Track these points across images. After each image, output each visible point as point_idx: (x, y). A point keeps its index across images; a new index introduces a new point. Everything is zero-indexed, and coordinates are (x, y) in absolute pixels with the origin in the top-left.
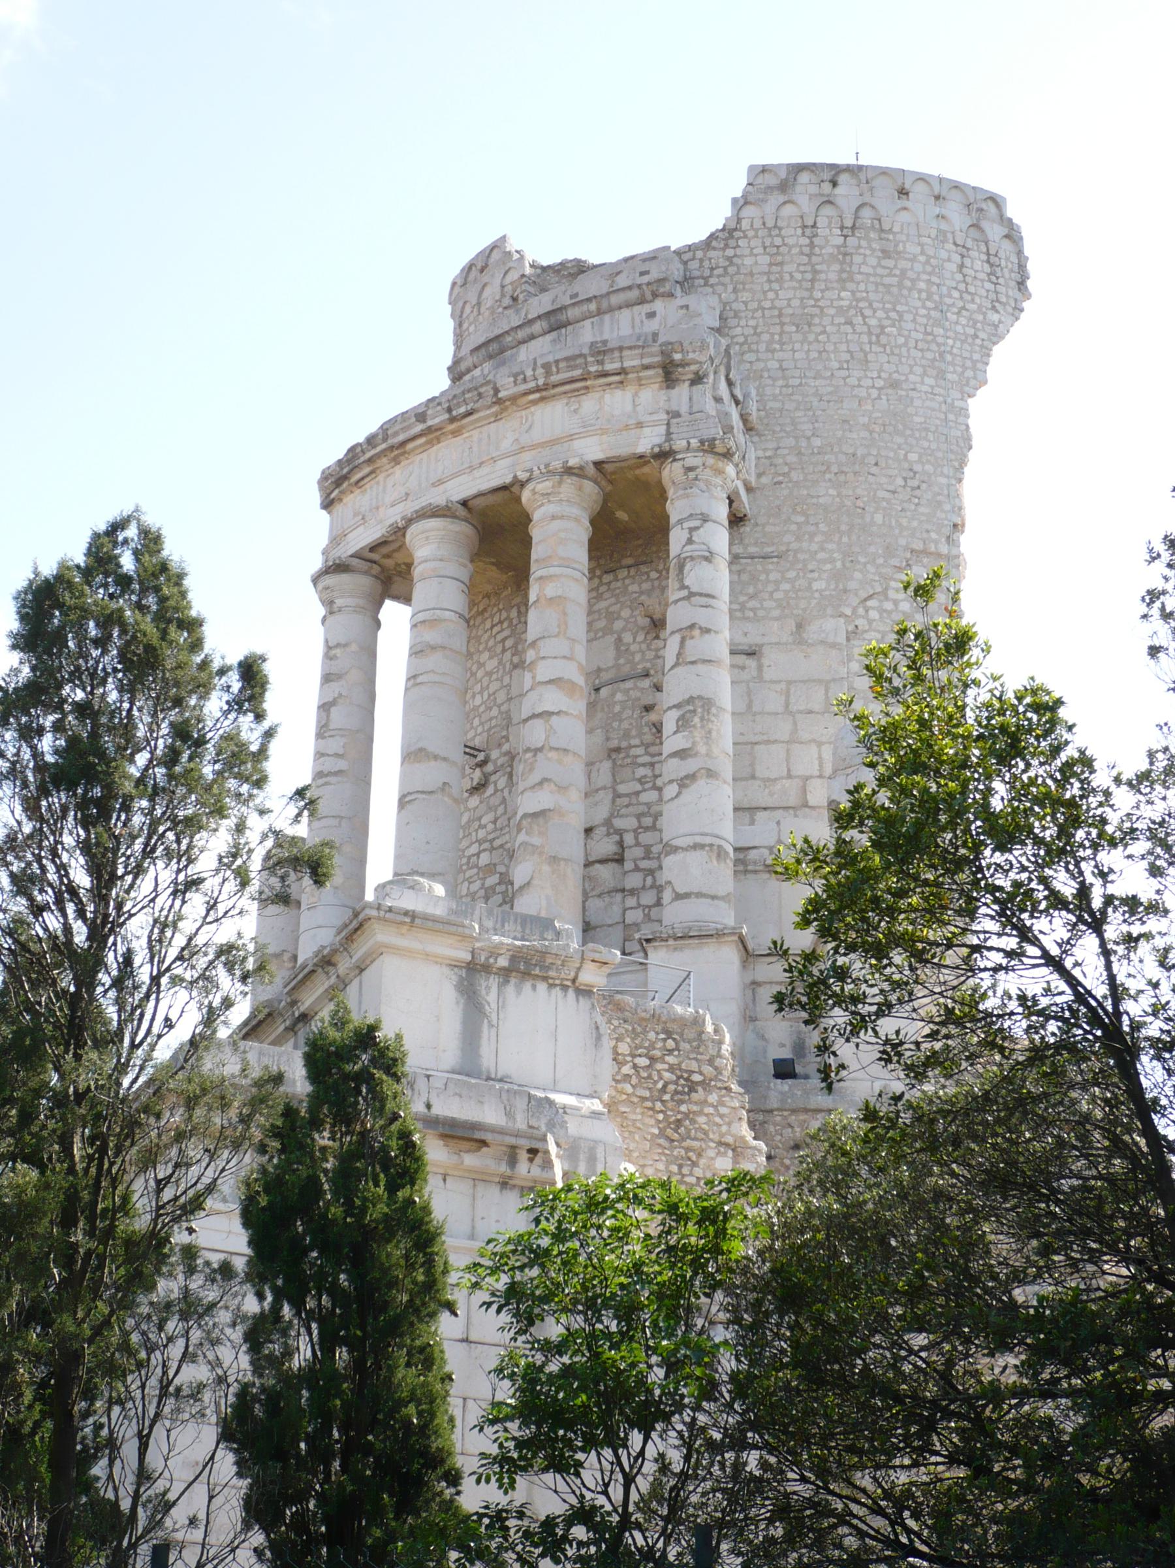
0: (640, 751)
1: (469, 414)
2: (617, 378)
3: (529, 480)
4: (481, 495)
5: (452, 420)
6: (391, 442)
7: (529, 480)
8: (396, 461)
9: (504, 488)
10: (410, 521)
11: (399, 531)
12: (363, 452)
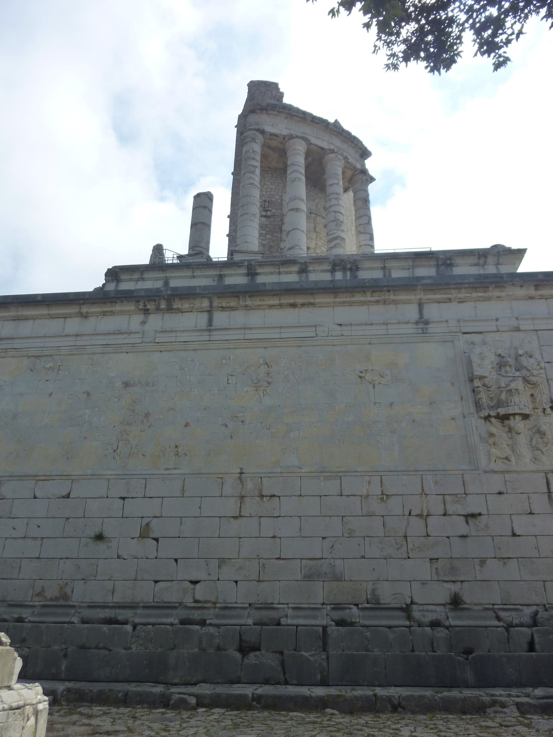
0: (322, 236)
1: (317, 123)
2: (353, 145)
3: (336, 153)
4: (316, 146)
5: (312, 121)
6: (290, 112)
7: (336, 153)
8: (286, 118)
9: (323, 149)
10: (297, 137)
11: (291, 137)
12: (279, 108)
